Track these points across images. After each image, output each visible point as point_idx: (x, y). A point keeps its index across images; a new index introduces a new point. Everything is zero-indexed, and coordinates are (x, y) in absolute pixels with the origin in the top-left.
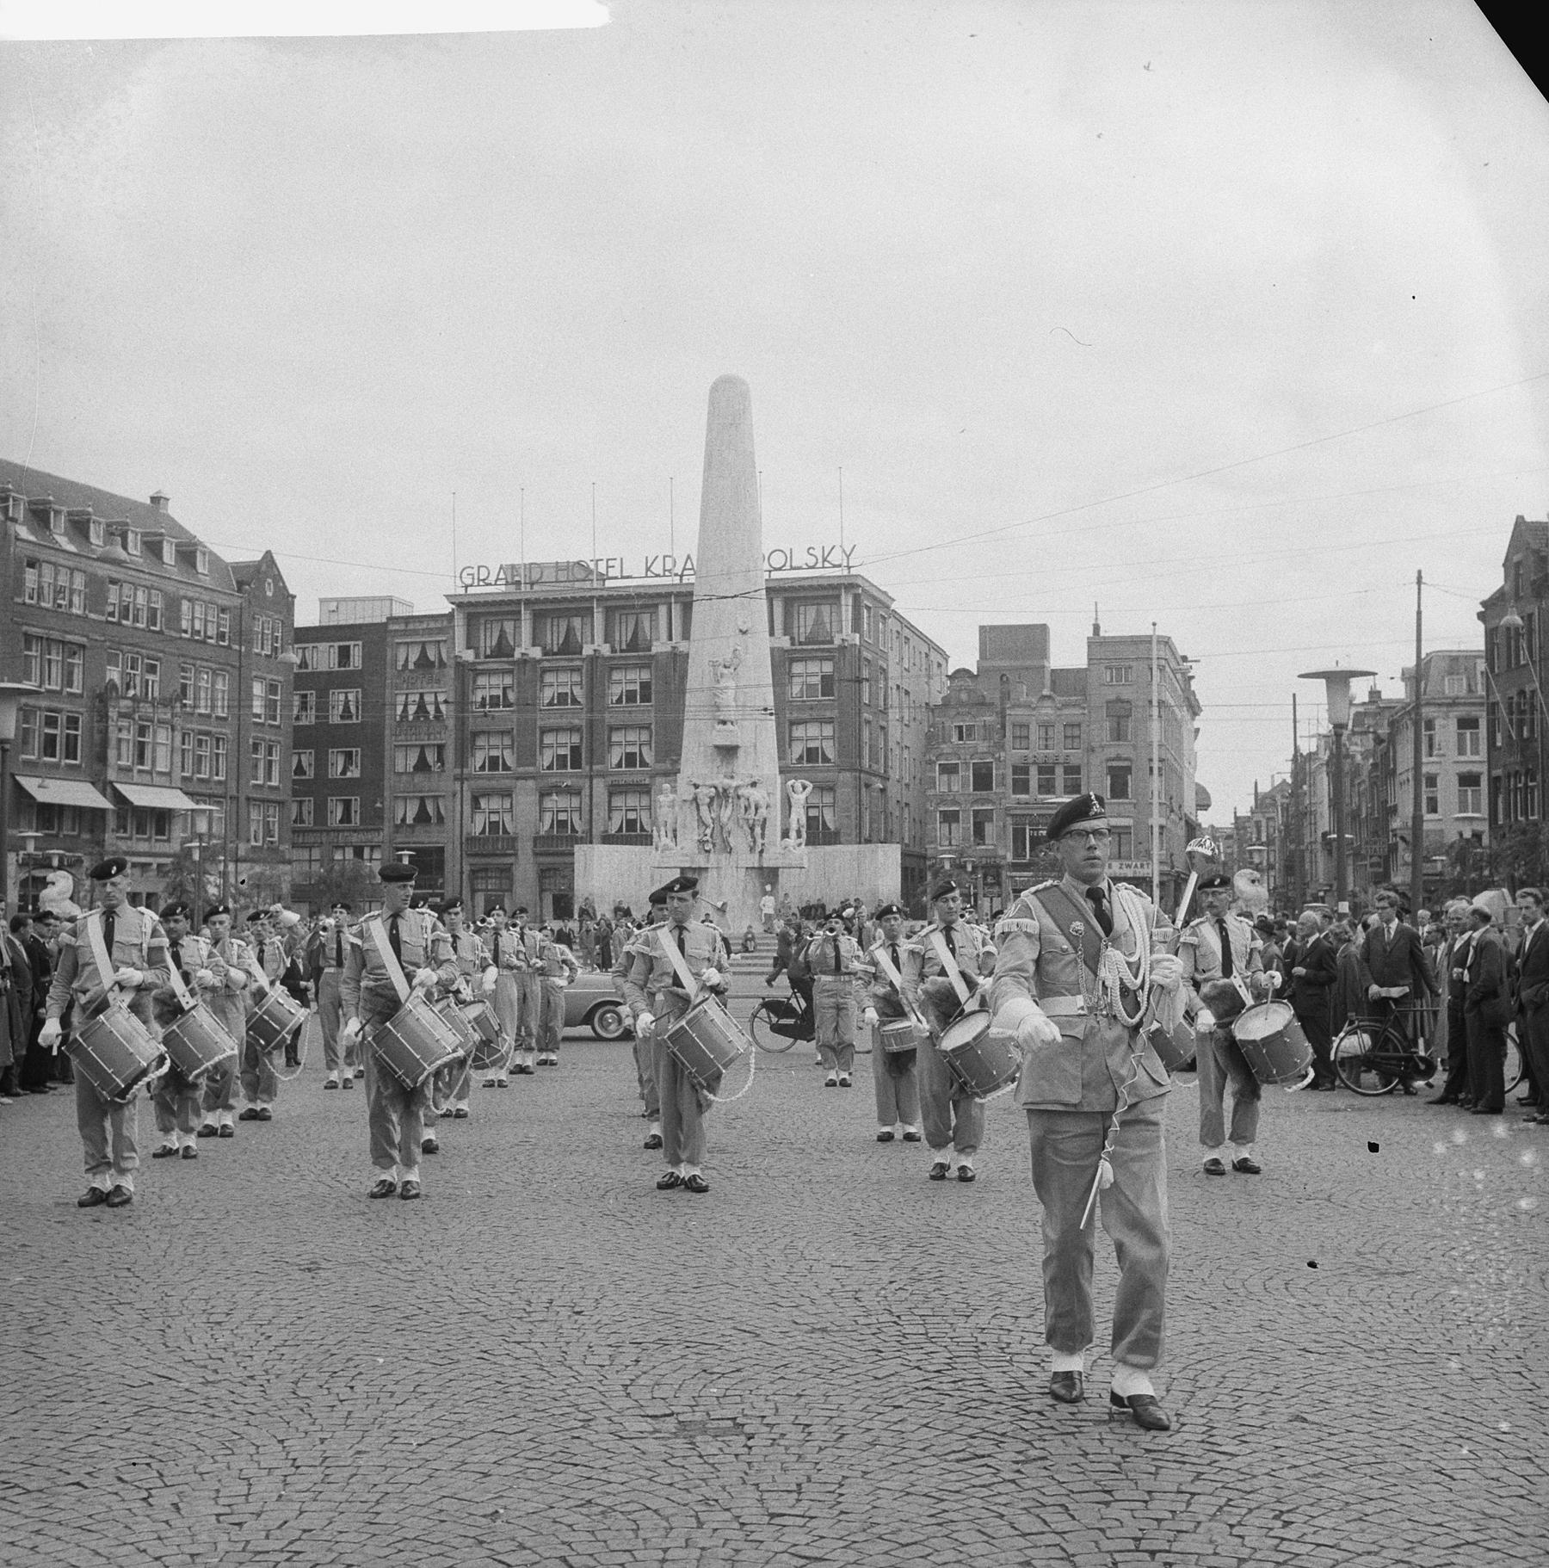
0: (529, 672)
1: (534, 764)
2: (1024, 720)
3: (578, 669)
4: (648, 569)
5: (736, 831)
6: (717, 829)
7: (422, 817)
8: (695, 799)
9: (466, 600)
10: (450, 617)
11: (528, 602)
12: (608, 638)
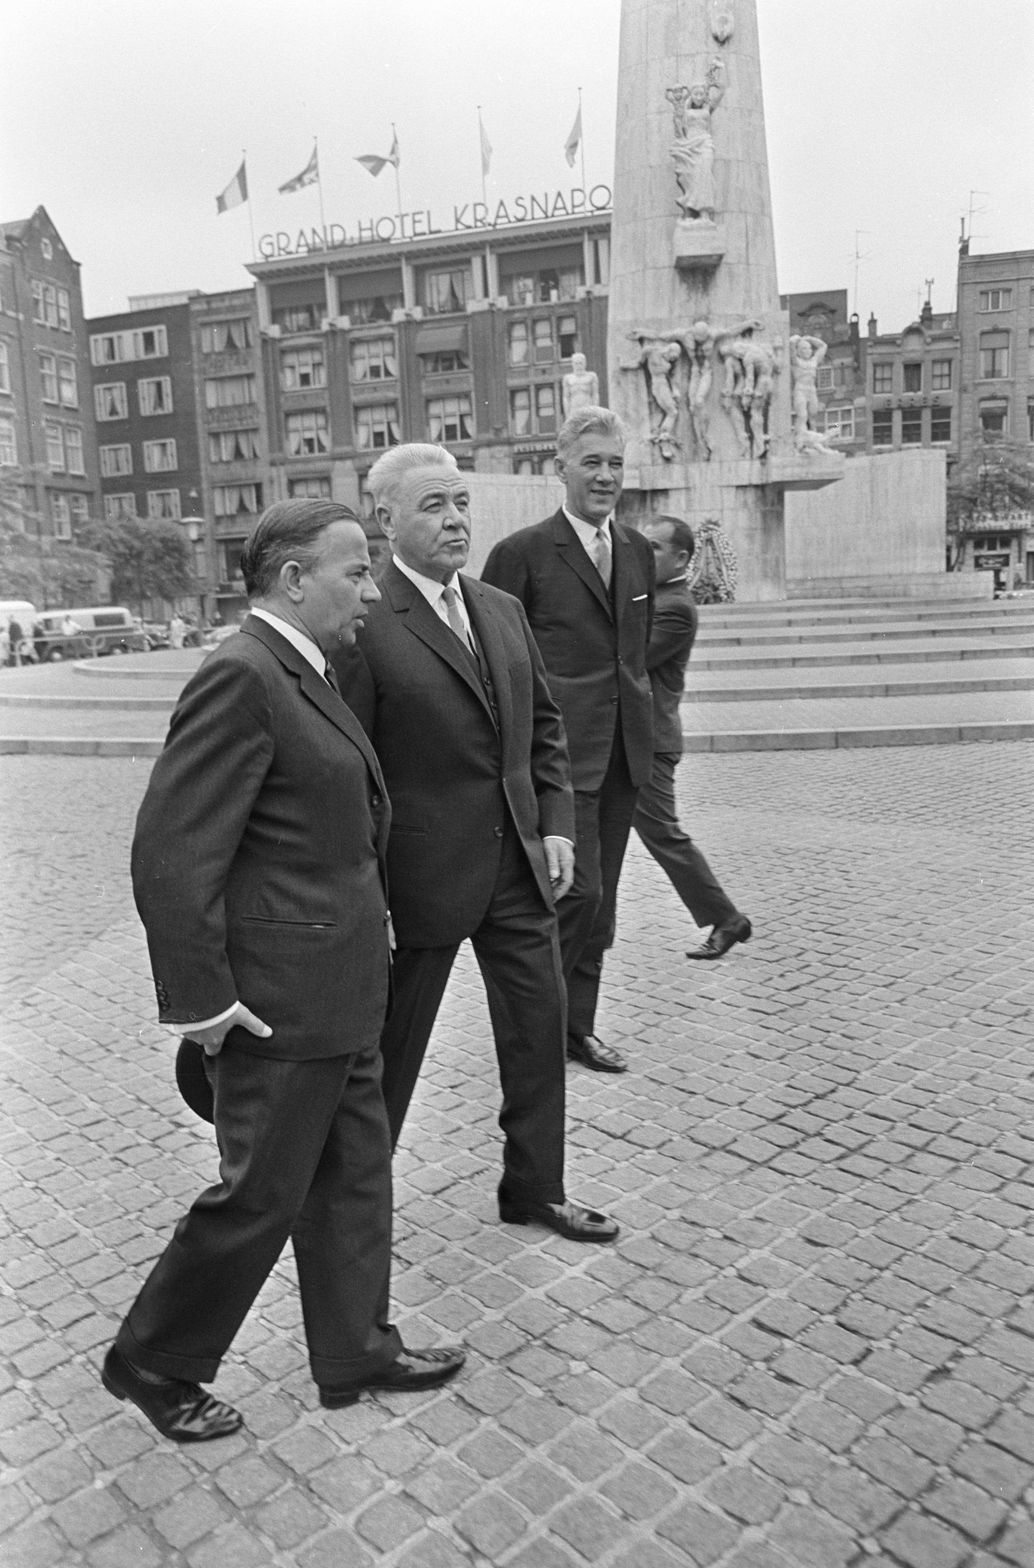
1: (350, 443)
2: (888, 359)
3: (390, 338)
4: (458, 221)
5: (719, 421)
6: (684, 416)
8: (644, 366)
9: (265, 269)
10: (252, 291)
11: (332, 267)
12: (419, 300)
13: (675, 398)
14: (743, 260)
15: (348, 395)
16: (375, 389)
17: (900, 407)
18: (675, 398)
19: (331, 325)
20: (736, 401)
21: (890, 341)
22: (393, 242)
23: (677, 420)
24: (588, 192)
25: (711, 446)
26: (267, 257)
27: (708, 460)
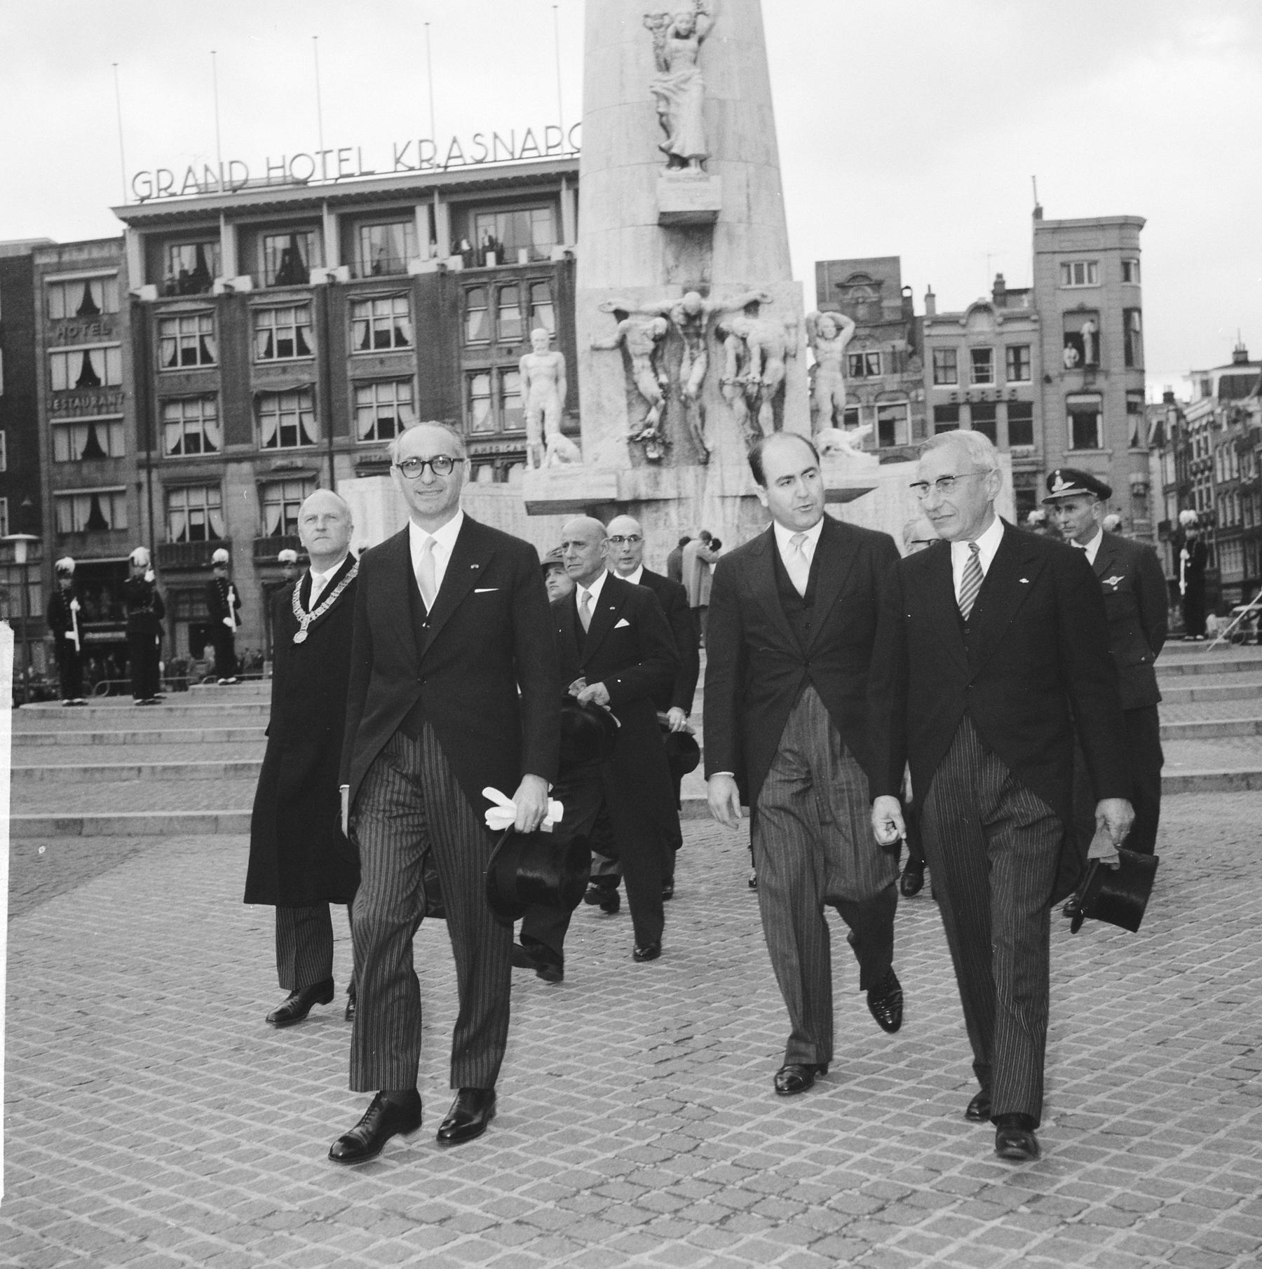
0: (236, 313)
1: (247, 440)
2: (950, 343)
4: (397, 161)
6: (675, 408)
7: (96, 522)
8: (622, 344)
9: (139, 213)
10: (120, 242)
11: (231, 214)
12: (345, 258)
13: (661, 386)
14: (744, 219)
15: (247, 376)
16: (284, 370)
17: (967, 402)
18: (661, 386)
19: (226, 286)
20: (739, 390)
21: (951, 320)
22: (310, 184)
23: (664, 413)
24: (566, 130)
25: (709, 445)
26: (143, 199)
27: (705, 463)
